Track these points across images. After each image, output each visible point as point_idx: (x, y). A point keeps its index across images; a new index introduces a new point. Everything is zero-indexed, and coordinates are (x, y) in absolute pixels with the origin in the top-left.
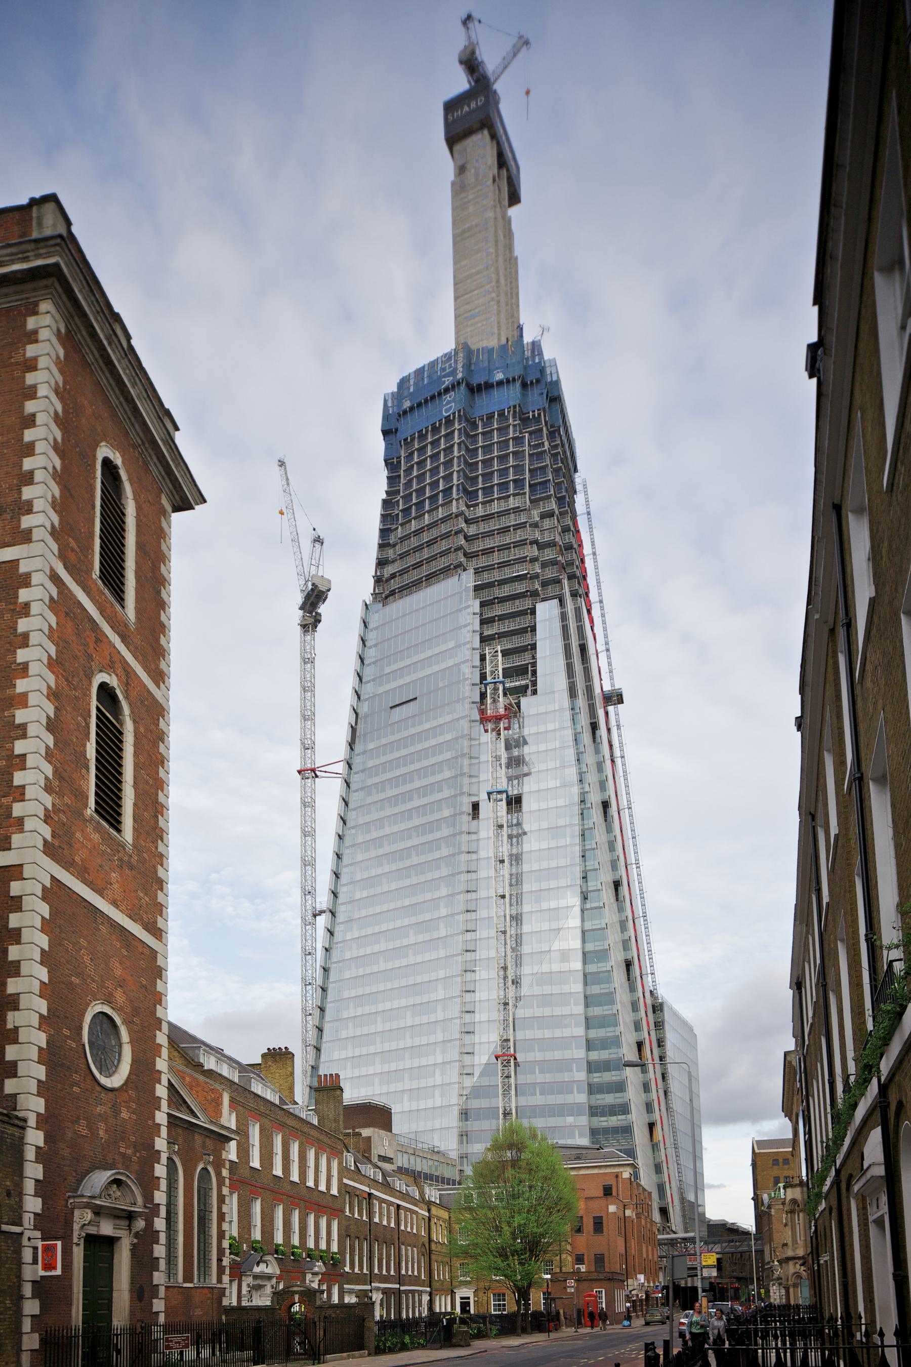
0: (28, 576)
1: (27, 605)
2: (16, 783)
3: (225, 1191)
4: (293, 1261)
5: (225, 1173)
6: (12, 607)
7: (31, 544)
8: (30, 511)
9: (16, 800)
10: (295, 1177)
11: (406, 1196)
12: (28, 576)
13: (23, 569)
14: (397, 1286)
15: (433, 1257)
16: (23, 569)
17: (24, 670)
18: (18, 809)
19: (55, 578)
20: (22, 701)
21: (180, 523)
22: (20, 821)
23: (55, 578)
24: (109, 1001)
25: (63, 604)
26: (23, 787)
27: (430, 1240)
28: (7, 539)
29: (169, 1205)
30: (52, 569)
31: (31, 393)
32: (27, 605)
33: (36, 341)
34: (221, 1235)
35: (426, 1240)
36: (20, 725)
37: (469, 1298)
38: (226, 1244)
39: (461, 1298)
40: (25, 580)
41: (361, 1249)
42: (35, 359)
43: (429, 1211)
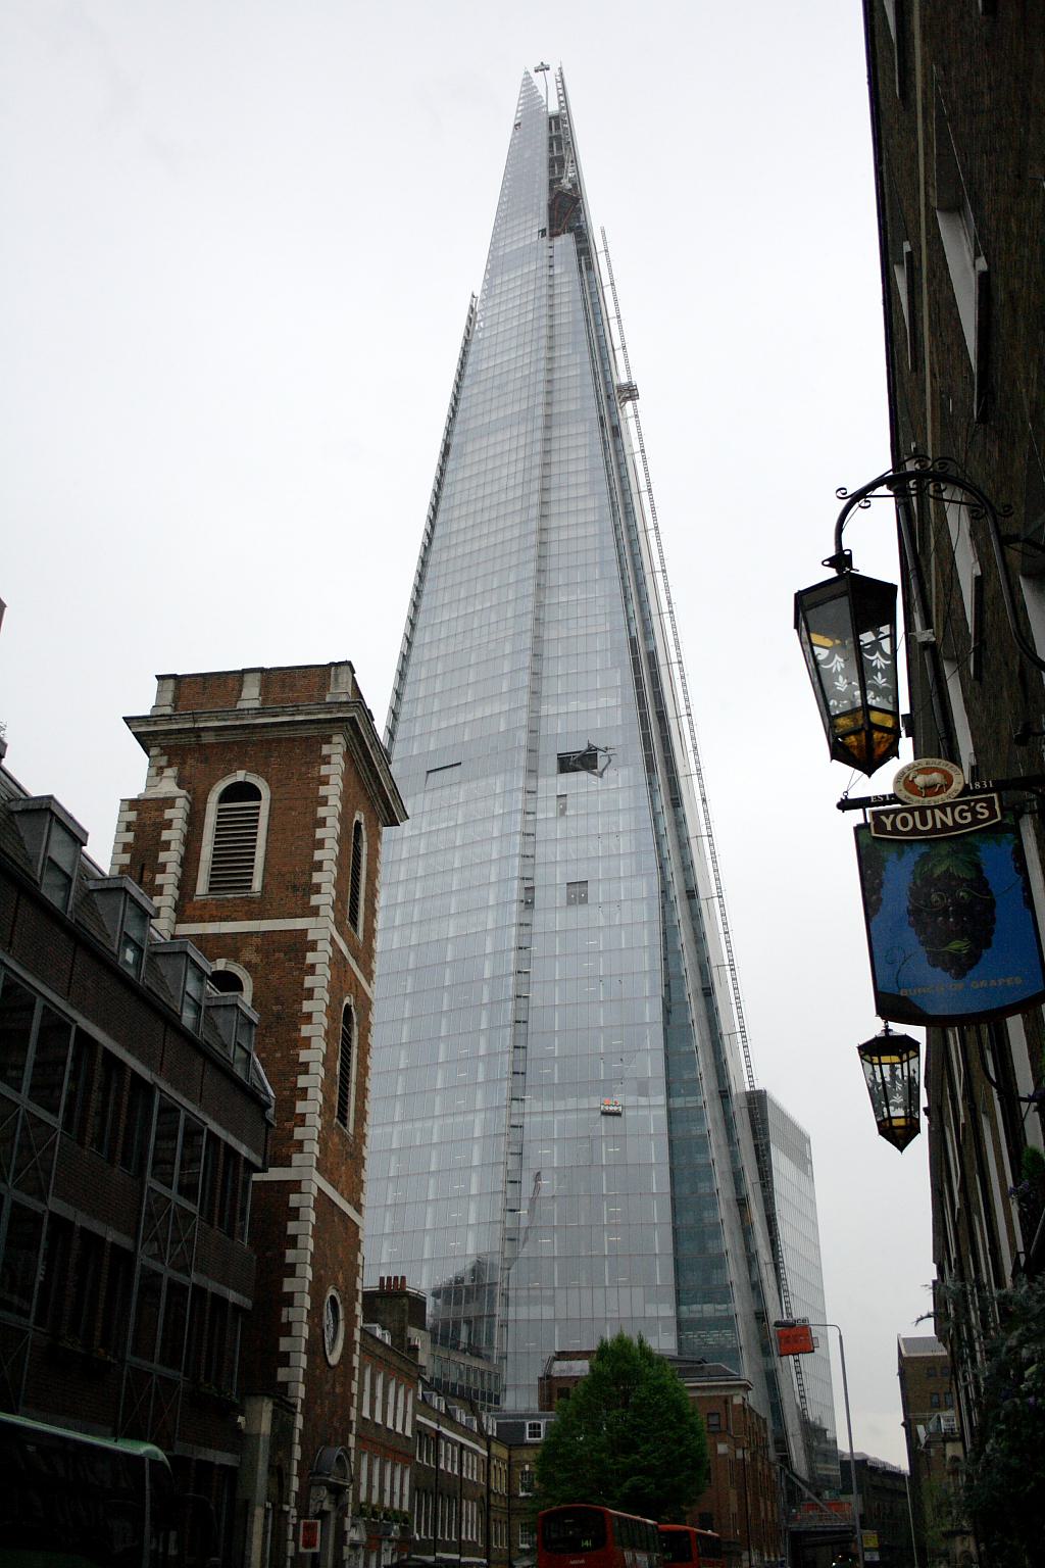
0: (315, 942)
1: (313, 966)
2: (297, 1111)
6: (300, 966)
7: (319, 918)
8: (318, 892)
9: (296, 1125)
11: (466, 1431)
12: (315, 942)
13: (311, 937)
14: (457, 1557)
15: (492, 1514)
16: (311, 937)
17: (308, 1017)
18: (299, 1134)
19: (333, 942)
20: (306, 1043)
22: (301, 1143)
23: (333, 942)
25: (338, 962)
26: (304, 1115)
27: (489, 1491)
28: (299, 911)
30: (332, 937)
31: (324, 801)
32: (313, 966)
33: (329, 763)
35: (485, 1491)
36: (302, 1063)
40: (313, 946)
41: (427, 1507)
42: (328, 776)
43: (489, 1450)
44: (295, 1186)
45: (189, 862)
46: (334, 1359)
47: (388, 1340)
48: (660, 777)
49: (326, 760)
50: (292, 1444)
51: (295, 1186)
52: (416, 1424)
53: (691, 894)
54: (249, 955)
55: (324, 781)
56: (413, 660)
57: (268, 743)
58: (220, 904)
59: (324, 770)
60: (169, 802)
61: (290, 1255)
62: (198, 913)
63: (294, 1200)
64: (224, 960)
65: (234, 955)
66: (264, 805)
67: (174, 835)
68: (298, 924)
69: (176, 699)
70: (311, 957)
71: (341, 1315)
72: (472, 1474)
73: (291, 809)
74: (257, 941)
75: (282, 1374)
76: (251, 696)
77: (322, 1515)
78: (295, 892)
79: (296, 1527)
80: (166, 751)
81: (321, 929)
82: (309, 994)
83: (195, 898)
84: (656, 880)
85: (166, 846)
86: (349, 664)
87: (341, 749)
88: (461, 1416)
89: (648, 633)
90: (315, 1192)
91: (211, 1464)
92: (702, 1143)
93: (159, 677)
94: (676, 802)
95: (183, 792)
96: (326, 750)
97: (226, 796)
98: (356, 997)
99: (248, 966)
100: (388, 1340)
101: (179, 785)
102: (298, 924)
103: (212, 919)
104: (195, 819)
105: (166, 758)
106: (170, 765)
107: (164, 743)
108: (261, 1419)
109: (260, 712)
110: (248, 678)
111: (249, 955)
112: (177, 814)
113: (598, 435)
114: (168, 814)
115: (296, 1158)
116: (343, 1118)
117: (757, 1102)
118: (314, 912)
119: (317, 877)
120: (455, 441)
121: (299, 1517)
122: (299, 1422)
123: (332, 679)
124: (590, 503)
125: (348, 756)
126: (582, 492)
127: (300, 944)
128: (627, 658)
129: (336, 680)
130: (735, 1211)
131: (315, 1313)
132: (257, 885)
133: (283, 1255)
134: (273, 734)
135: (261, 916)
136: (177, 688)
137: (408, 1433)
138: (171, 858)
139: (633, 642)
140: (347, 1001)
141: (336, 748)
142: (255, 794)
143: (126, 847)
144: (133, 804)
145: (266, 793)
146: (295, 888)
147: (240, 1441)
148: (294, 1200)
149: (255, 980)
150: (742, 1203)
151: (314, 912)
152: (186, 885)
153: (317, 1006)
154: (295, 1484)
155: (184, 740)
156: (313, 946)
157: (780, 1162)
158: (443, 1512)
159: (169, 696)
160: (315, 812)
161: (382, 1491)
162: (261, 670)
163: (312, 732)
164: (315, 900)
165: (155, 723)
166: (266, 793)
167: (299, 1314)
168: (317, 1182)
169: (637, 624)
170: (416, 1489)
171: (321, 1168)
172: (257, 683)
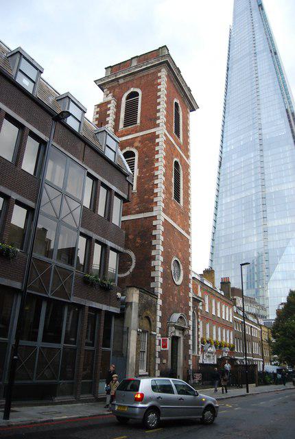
3: (199, 320)
4: (219, 346)
5: (199, 314)
10: (219, 316)
11: (253, 323)
21: (192, 115)
23: (165, 135)
24: (177, 257)
25: (167, 142)
29: (193, 325)
34: (198, 336)
38: (200, 340)
44: (155, 218)
45: (117, 120)
46: (179, 282)
47: (223, 294)
49: (160, 78)
50: (156, 310)
51: (155, 218)
52: (233, 319)
56: (225, 126)
60: (109, 102)
61: (154, 242)
63: (155, 223)
66: (140, 97)
67: (111, 112)
68: (152, 131)
70: (157, 140)
71: (181, 268)
72: (256, 334)
74: (139, 139)
75: (152, 285)
77: (175, 339)
78: (151, 121)
79: (160, 340)
80: (109, 89)
85: (109, 115)
86: (165, 46)
88: (251, 318)
90: (163, 220)
91: (99, 310)
93: (106, 68)
96: (159, 74)
97: (128, 97)
98: (181, 161)
99: (136, 148)
100: (223, 294)
101: (113, 96)
102: (152, 131)
104: (118, 107)
108: (134, 296)
109: (136, 67)
111: (137, 144)
112: (112, 106)
113: (270, 55)
114: (109, 106)
115: (155, 209)
116: (177, 197)
118: (158, 125)
120: (230, 66)
121: (162, 337)
122: (160, 302)
125: (168, 76)
127: (154, 136)
128: (286, 114)
131: (166, 263)
133: (151, 242)
137: (231, 321)
138: (111, 119)
139: (287, 110)
140: (175, 159)
141: (163, 73)
142: (136, 94)
143: (97, 119)
144: (99, 106)
145: (140, 93)
146: (151, 120)
147: (125, 305)
148: (155, 223)
151: (158, 125)
152: (116, 128)
153: (161, 156)
154: (159, 325)
158: (222, 334)
161: (222, 338)
166: (140, 93)
167: (158, 264)
168: (163, 217)
170: (235, 337)
171: (164, 211)
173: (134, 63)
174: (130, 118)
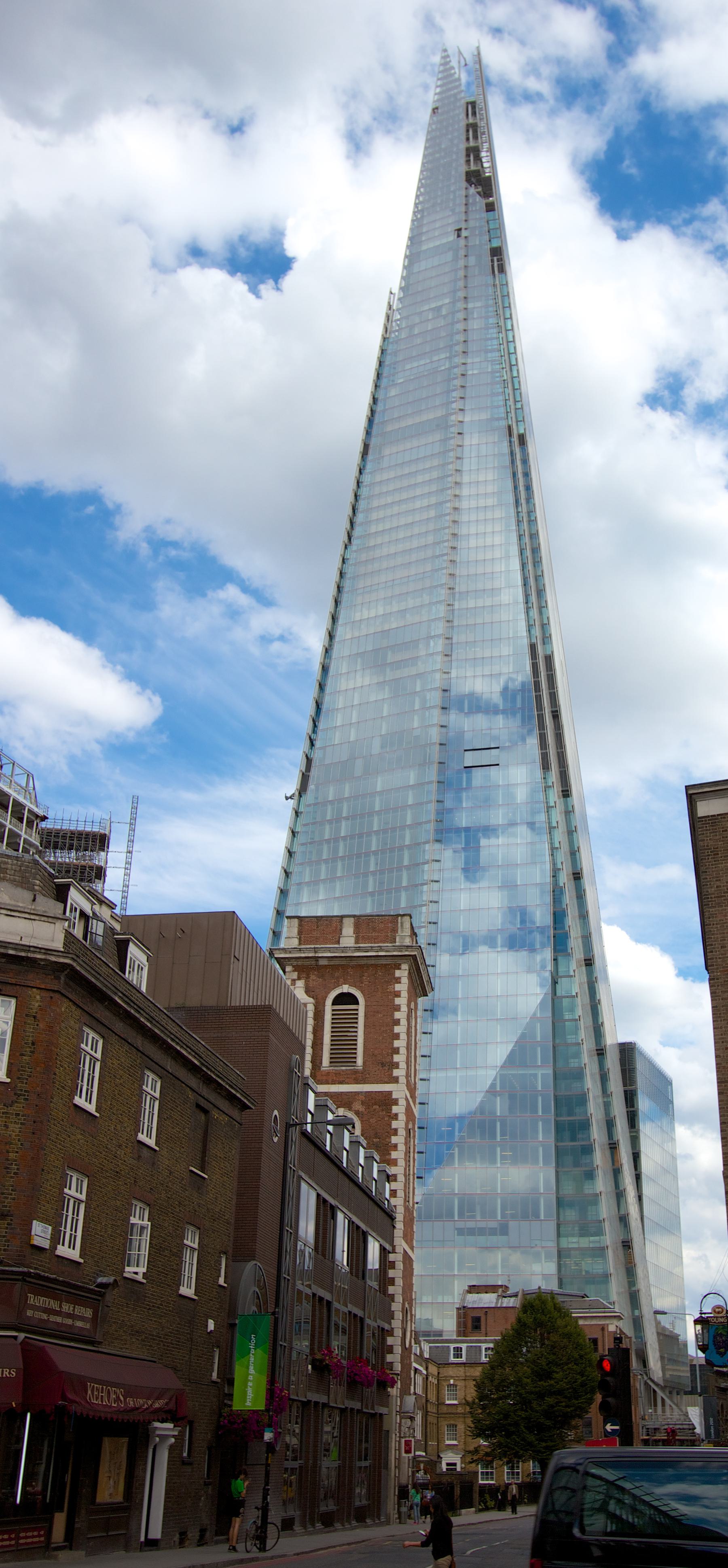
13: (394, 1096)
16: (394, 1096)
37: (455, 1464)
39: (448, 1464)
40: (396, 1102)
48: (554, 776)
49: (398, 980)
53: (577, 876)
54: (358, 1106)
55: (398, 994)
57: (361, 966)
58: (338, 1074)
59: (397, 987)
62: (324, 1078)
64: (342, 1109)
65: (348, 1106)
69: (300, 933)
70: (395, 1109)
73: (378, 1012)
74: (362, 1097)
76: (348, 938)
78: (382, 1065)
80: (296, 968)
81: (399, 1091)
82: (395, 1132)
83: (322, 1069)
84: (548, 867)
87: (406, 973)
89: (546, 638)
92: (582, 1099)
94: (566, 793)
95: (311, 1000)
96: (398, 973)
99: (357, 1113)
101: (308, 991)
103: (334, 1083)
105: (296, 973)
106: (299, 978)
107: (295, 963)
110: (345, 920)
111: (358, 1106)
117: (627, 1051)
118: (396, 1080)
119: (396, 1058)
123: (399, 925)
124: (498, 514)
126: (490, 502)
127: (387, 1100)
129: (402, 926)
130: (608, 1153)
132: (360, 1061)
134: (363, 962)
135: (364, 1081)
136: (300, 925)
139: (533, 647)
141: (403, 973)
142: (353, 1000)
146: (383, 1065)
149: (362, 1122)
150: (613, 1147)
151: (396, 1080)
155: (307, 963)
156: (396, 1102)
157: (643, 1104)
159: (296, 930)
160: (393, 1015)
162: (354, 916)
163: (389, 962)
164: (396, 1072)
165: (290, 952)
169: (537, 632)
172: (352, 925)
173: (348, 930)
174: (343, 1049)
